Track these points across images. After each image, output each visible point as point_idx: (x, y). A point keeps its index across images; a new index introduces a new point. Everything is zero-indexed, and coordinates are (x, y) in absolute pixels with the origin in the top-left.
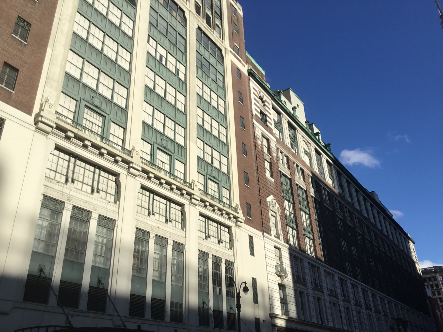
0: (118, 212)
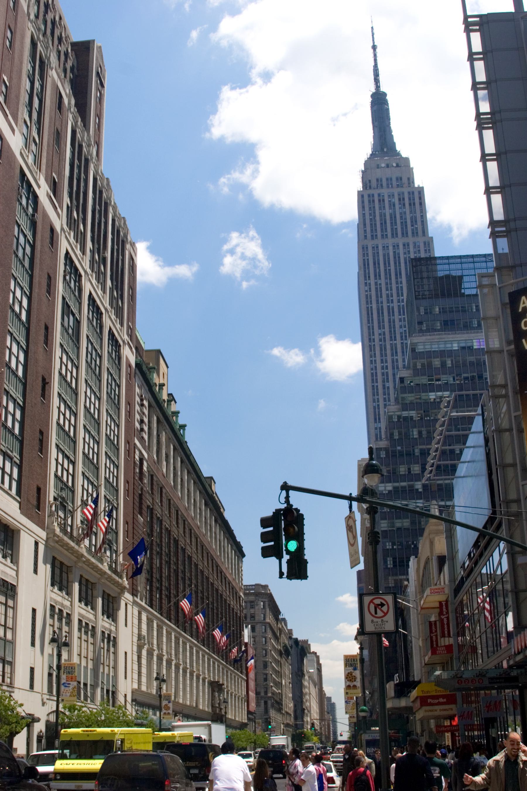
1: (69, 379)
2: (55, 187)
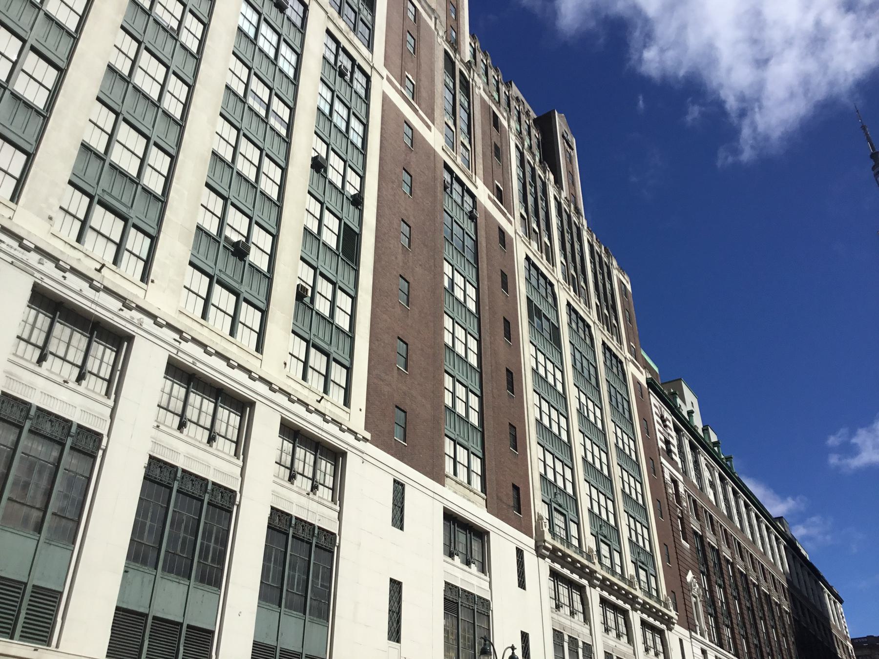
0: (591, 634)
1: (627, 451)
2: (500, 195)
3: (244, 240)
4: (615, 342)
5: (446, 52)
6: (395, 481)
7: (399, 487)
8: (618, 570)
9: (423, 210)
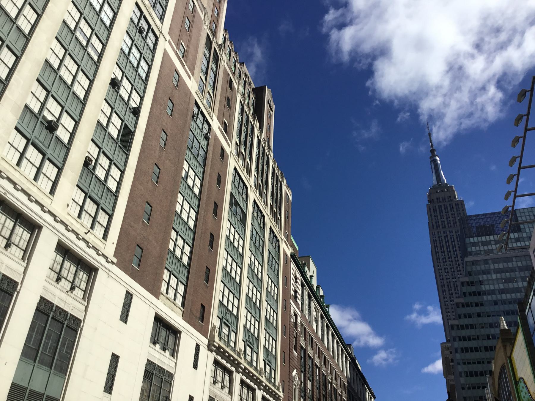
2: (226, 128)
3: (55, 120)
4: (277, 229)
5: (208, 35)
6: (127, 292)
7: (129, 297)
8: (254, 364)
9: (177, 127)
